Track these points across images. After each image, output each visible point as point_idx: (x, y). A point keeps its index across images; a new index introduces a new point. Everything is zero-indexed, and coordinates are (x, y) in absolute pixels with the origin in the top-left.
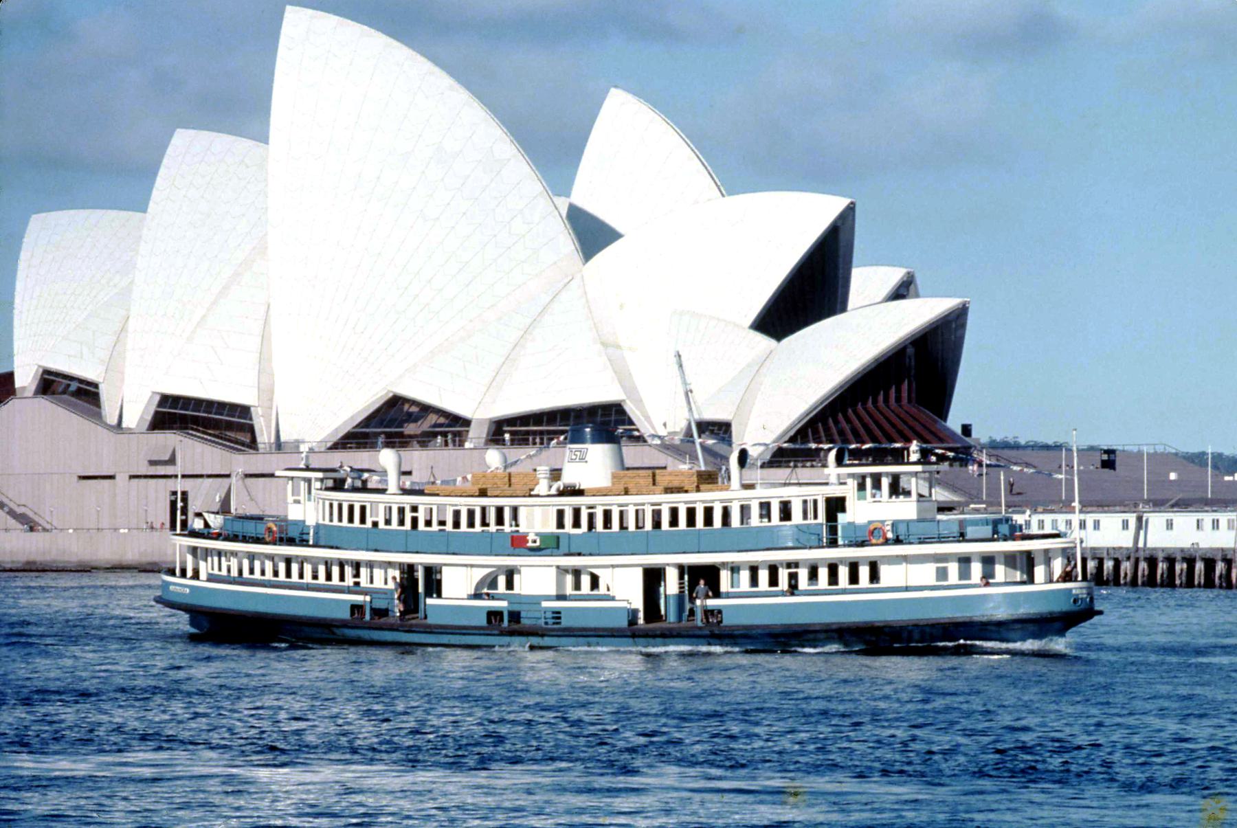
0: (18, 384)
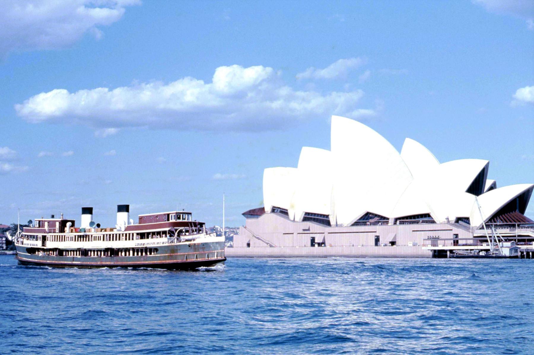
0: (266, 210)
